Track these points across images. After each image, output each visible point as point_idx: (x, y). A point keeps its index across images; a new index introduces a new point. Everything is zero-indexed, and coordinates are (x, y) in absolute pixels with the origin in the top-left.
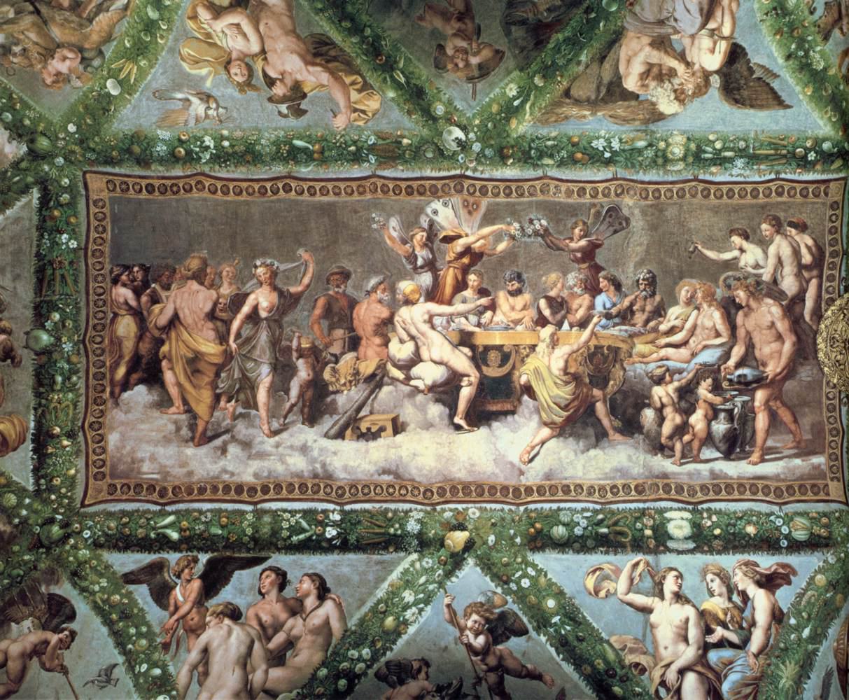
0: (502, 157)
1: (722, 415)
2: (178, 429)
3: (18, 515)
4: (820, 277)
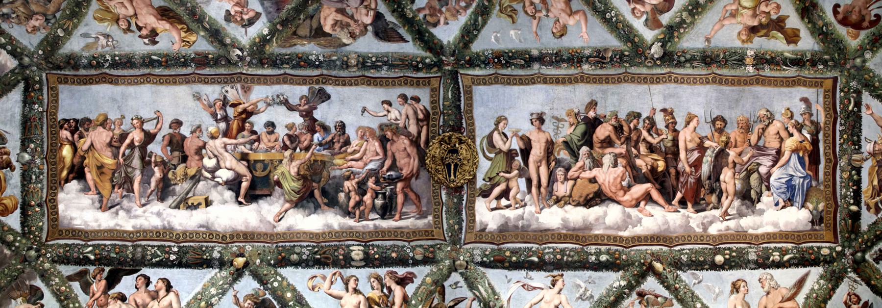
0: (261, 64)
2: (93, 203)
3: (14, 246)
4: (428, 125)
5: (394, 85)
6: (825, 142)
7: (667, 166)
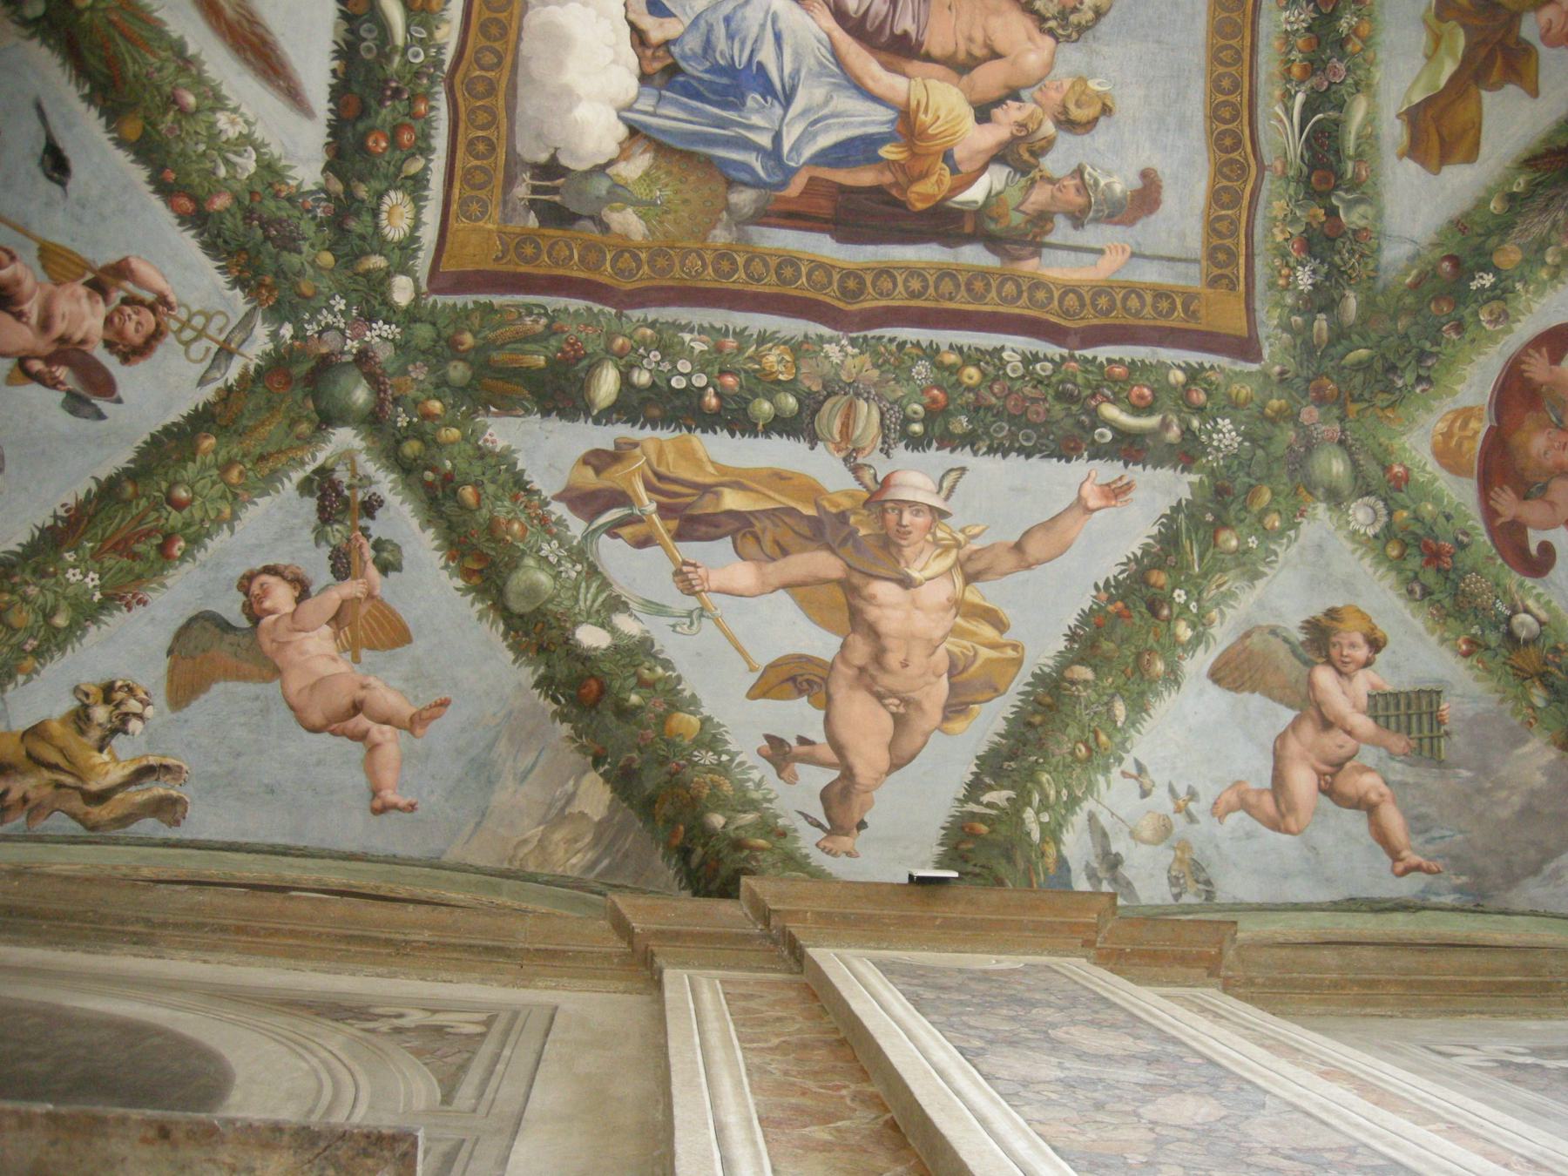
6: (946, 273)
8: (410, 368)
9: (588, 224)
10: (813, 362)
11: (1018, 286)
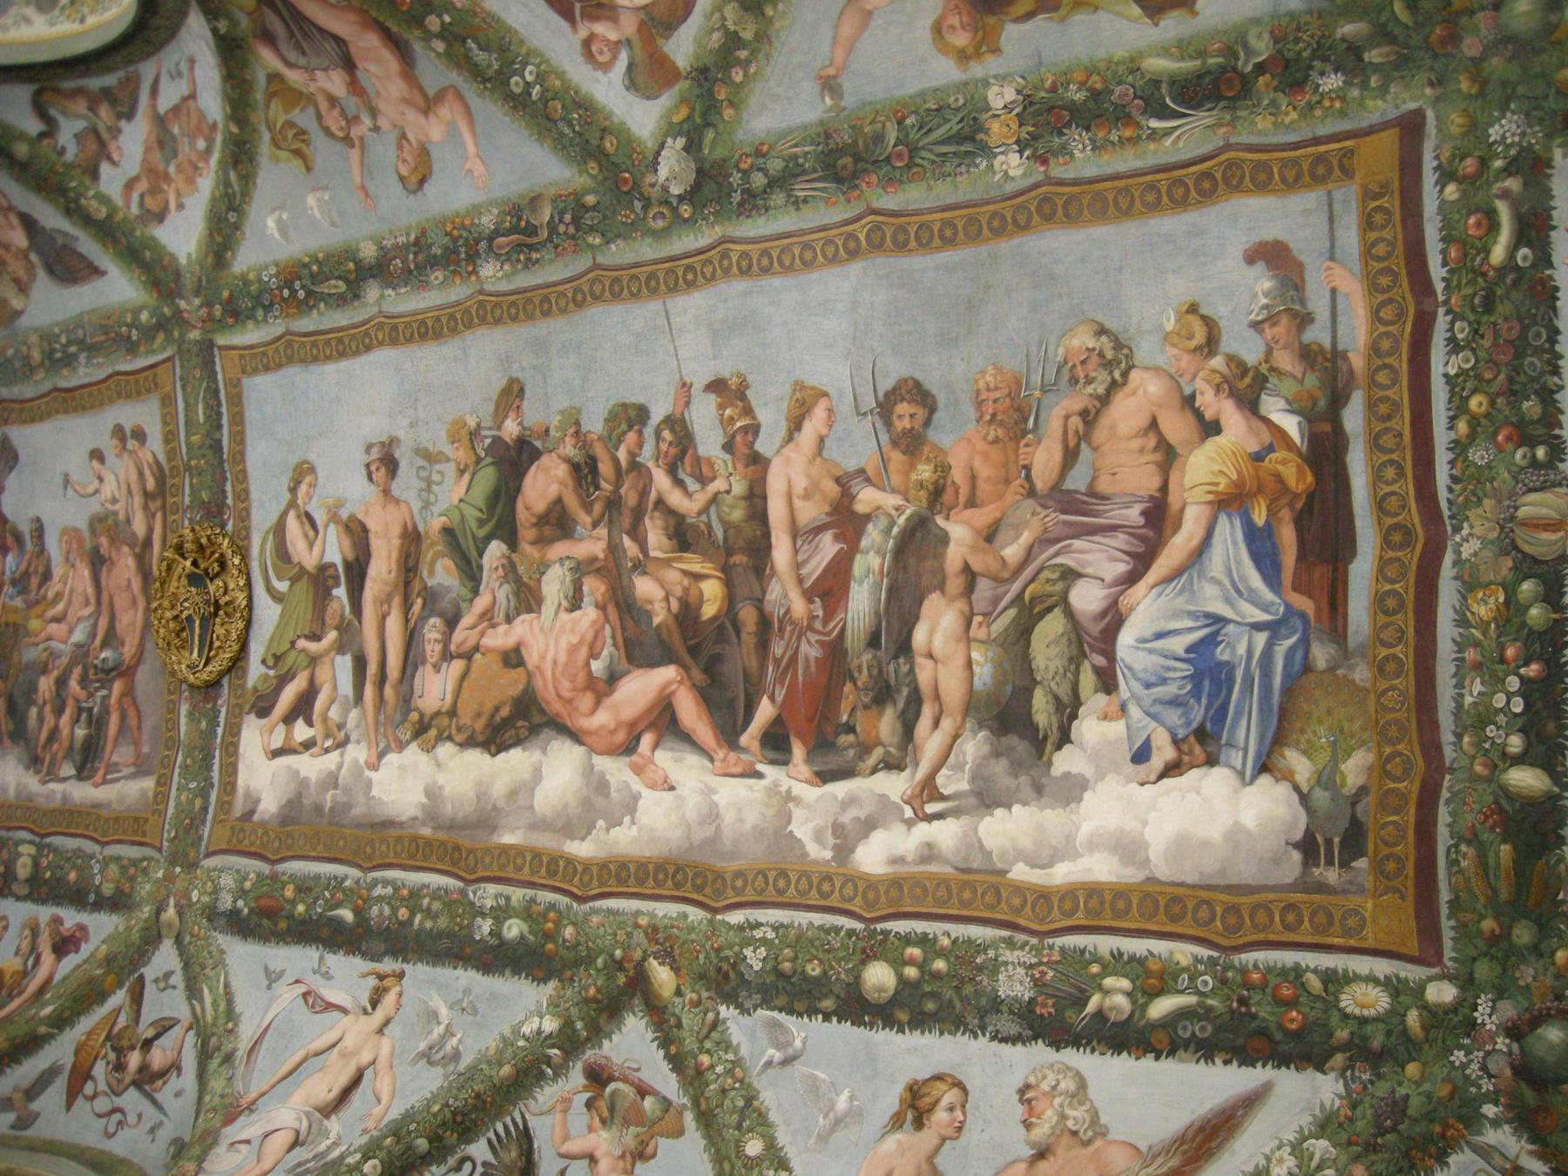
1: (84, 716)
4: (163, 508)
5: (102, 404)
6: (1375, 443)
7: (731, 600)
8: (1522, 983)
9: (1360, 808)
10: (1482, 568)
11: (1380, 368)
